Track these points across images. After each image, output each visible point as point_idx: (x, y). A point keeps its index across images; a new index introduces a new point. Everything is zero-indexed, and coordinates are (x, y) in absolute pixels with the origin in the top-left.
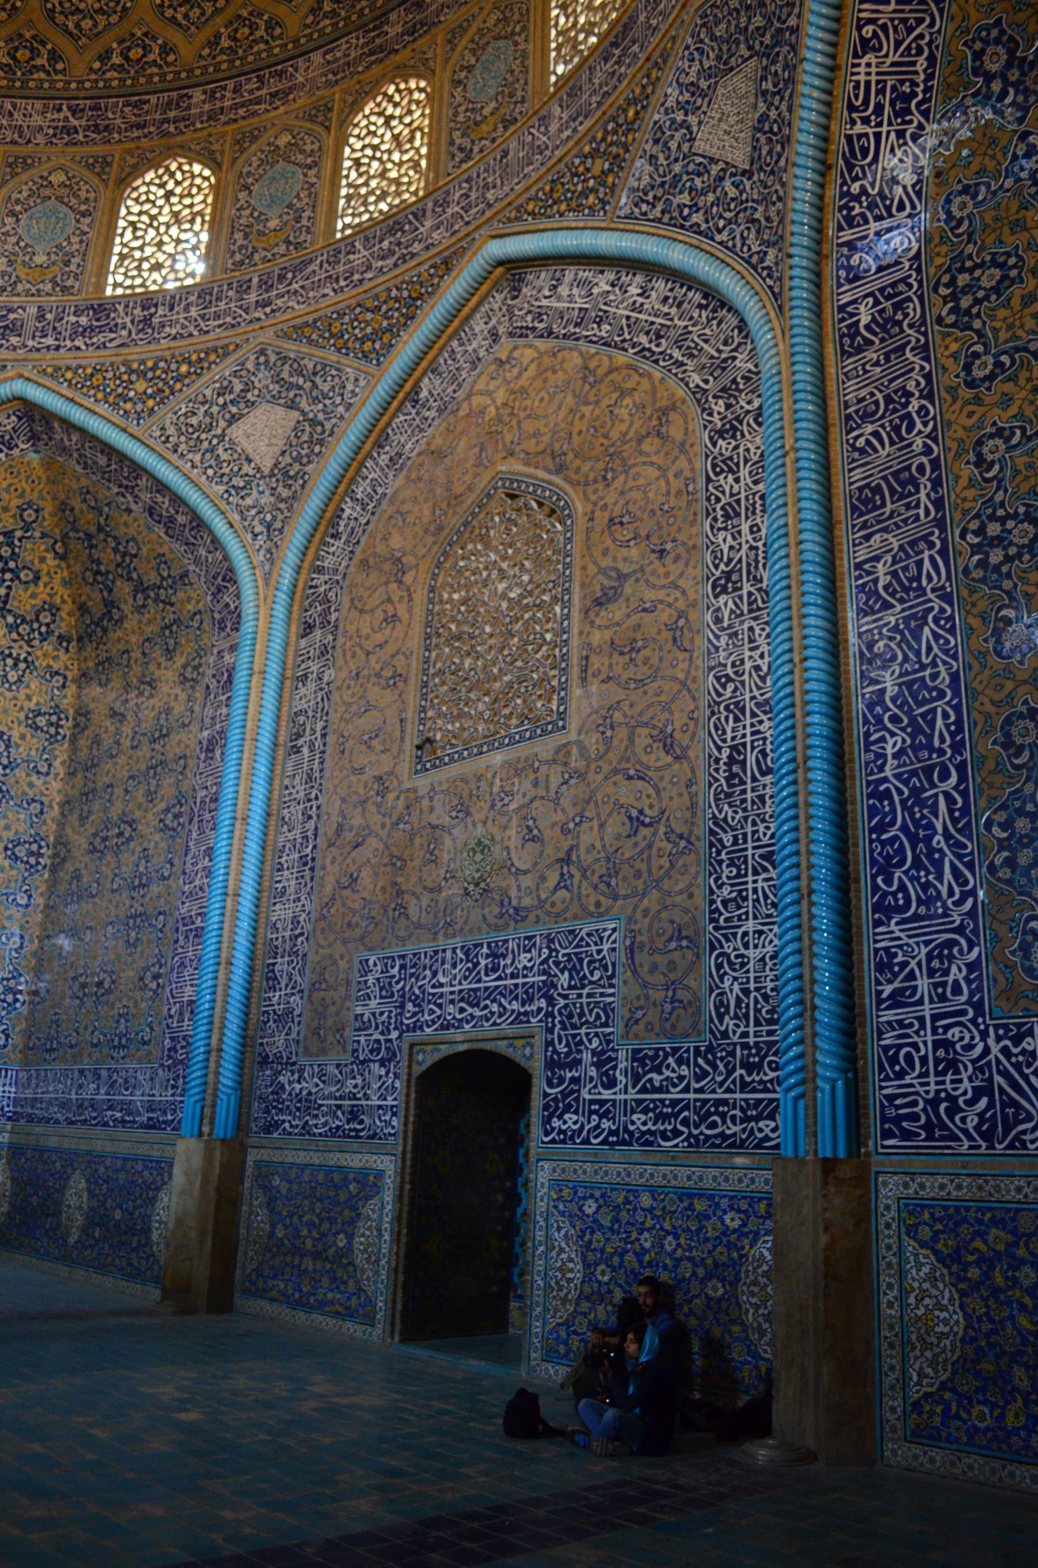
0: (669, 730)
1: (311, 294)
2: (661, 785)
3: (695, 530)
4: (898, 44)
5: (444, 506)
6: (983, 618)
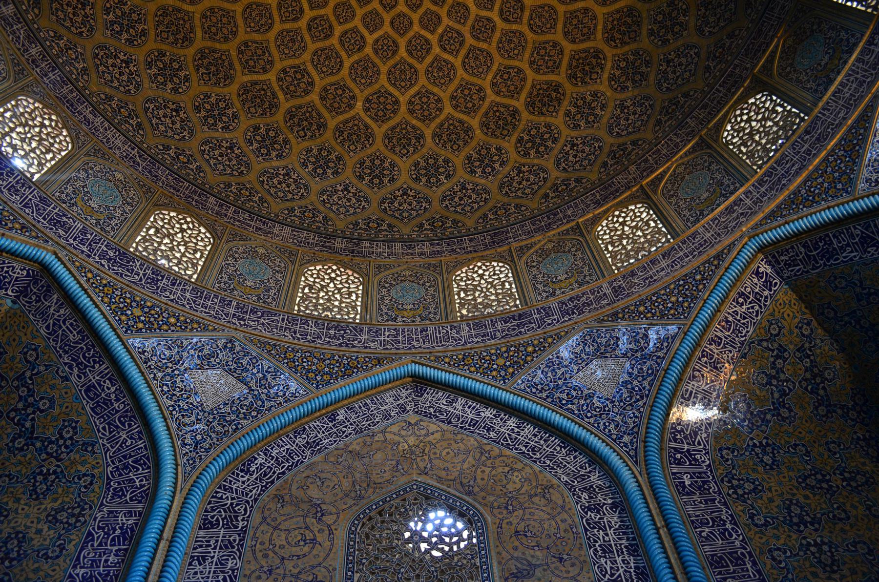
1: (275, 330)
5: (365, 485)
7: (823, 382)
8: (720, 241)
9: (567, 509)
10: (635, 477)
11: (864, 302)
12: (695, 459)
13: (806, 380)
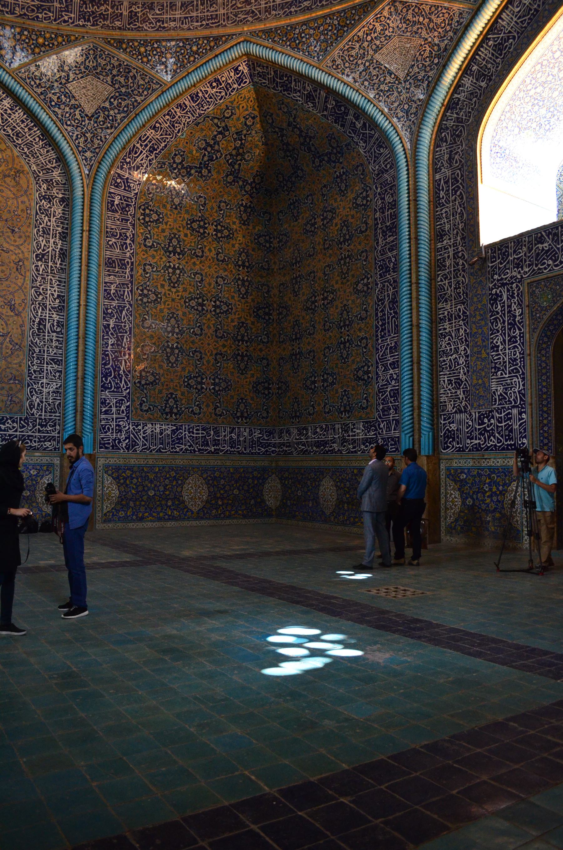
0: (13, 302)
2: (9, 322)
3: (29, 230)
4: (161, 135)
6: (140, 315)
7: (241, 160)
8: (225, 26)
9: (28, 193)
10: (83, 187)
11: (291, 129)
12: (129, 187)
13: (231, 155)
